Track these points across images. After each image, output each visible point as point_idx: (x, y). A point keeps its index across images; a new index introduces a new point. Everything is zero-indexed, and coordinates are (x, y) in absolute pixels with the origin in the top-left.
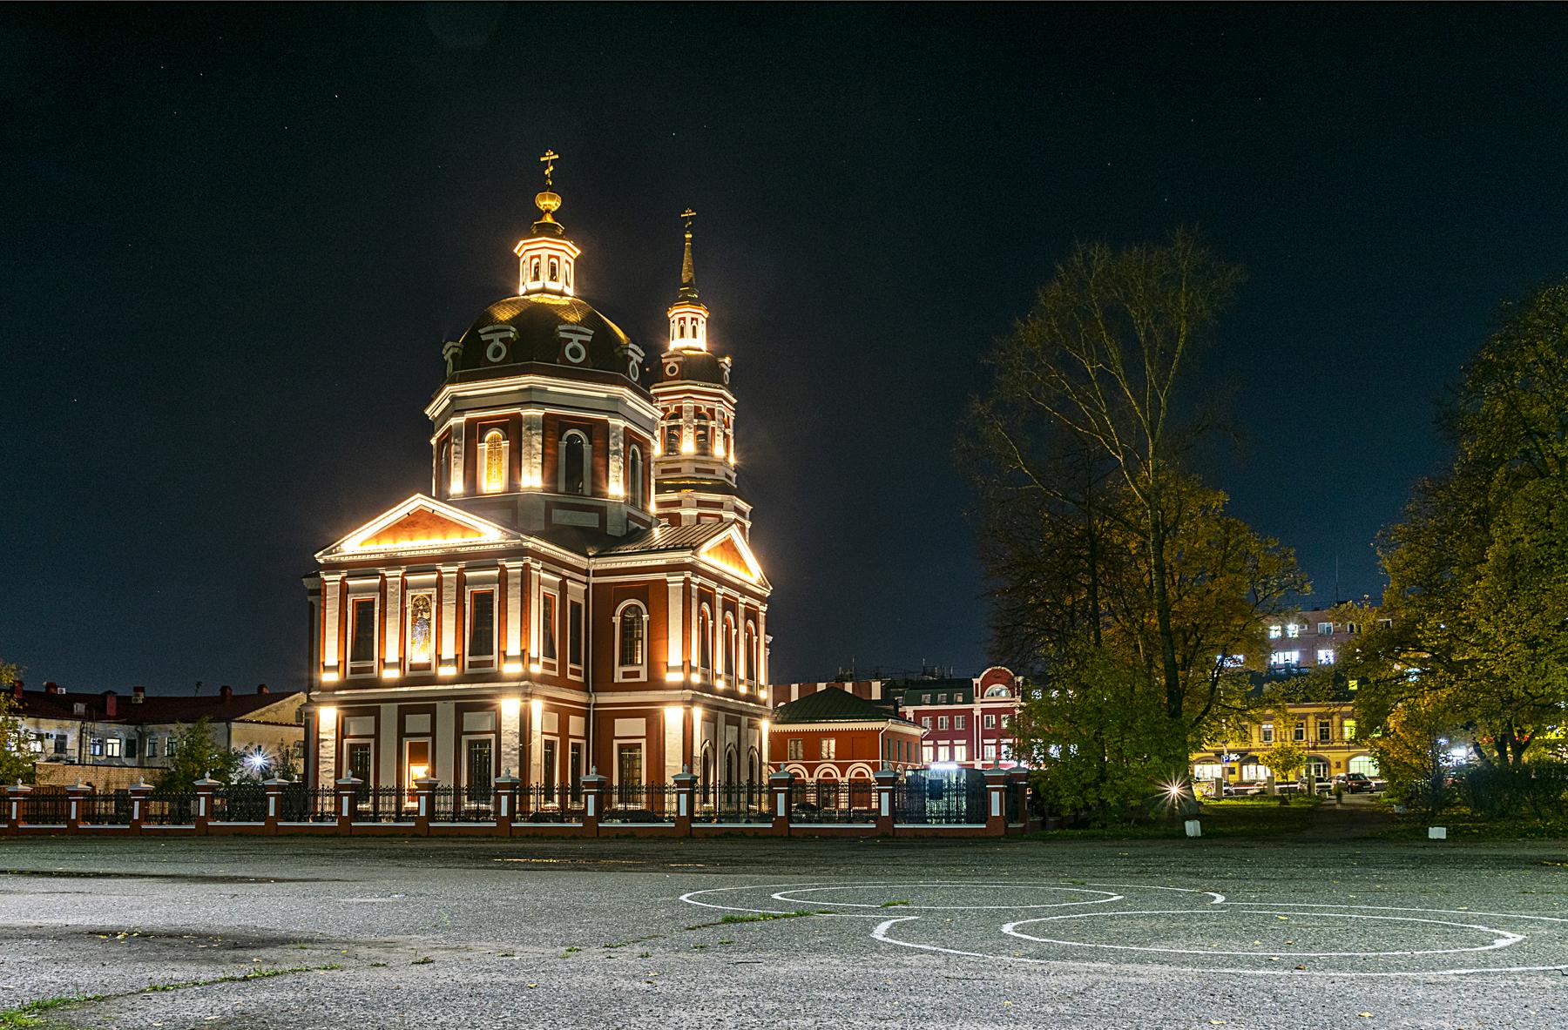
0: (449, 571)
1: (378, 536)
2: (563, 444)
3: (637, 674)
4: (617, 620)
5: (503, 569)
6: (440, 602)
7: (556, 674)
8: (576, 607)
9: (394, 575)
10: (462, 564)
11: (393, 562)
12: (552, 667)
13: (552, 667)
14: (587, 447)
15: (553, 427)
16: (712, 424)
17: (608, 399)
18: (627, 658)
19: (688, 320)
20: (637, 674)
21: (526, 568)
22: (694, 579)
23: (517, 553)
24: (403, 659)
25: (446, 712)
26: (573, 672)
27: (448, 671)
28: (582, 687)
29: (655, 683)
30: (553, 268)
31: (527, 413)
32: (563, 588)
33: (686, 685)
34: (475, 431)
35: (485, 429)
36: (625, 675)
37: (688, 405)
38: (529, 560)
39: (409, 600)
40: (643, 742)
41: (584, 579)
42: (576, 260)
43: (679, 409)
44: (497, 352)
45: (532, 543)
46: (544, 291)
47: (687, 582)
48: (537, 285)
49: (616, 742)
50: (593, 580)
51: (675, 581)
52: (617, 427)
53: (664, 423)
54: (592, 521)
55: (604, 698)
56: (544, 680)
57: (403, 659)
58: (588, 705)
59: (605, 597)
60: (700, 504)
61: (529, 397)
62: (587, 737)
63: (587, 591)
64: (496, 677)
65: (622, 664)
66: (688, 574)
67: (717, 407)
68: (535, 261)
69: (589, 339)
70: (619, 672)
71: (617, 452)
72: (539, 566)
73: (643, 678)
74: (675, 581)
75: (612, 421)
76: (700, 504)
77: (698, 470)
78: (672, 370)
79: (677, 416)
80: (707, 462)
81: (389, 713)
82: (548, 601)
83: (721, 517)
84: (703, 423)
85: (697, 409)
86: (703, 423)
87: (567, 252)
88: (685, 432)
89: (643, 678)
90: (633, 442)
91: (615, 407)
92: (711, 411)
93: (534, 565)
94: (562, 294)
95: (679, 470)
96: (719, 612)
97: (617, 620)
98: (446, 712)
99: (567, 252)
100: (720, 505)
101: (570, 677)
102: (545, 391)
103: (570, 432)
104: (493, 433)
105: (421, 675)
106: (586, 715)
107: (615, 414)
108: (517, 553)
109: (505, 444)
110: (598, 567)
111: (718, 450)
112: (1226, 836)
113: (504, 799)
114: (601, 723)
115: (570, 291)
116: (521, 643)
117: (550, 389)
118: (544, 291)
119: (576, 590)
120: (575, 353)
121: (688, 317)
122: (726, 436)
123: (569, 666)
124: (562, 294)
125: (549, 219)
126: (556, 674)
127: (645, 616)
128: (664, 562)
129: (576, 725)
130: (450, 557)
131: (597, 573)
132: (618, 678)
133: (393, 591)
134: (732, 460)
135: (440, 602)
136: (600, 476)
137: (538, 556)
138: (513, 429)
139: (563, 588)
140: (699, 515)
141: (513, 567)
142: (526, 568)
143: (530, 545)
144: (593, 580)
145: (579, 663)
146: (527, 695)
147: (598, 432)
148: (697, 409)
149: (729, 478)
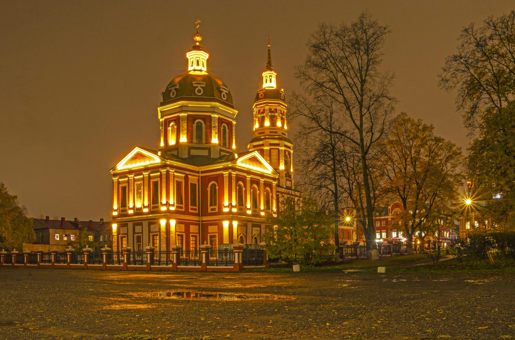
0: (146, 174)
1: (127, 164)
2: (195, 125)
5: (161, 172)
6: (144, 186)
7: (183, 210)
8: (193, 186)
9: (131, 176)
10: (149, 171)
11: (131, 172)
12: (182, 208)
13: (182, 208)
14: (204, 126)
15: (191, 119)
16: (276, 114)
17: (211, 107)
18: (213, 203)
19: (268, 77)
20: (214, 209)
21: (168, 172)
22: (233, 173)
23: (164, 166)
24: (134, 206)
25: (145, 224)
26: (191, 209)
27: (146, 210)
28: (197, 215)
30: (198, 62)
31: (182, 115)
32: (186, 178)
33: (230, 212)
34: (167, 123)
35: (170, 122)
36: (212, 210)
37: (267, 108)
38: (168, 168)
39: (135, 185)
40: (217, 234)
41: (198, 175)
42: (207, 60)
43: (264, 110)
44: (174, 93)
45: (169, 162)
46: (195, 70)
47: (230, 174)
48: (192, 68)
49: (209, 235)
50: (201, 175)
51: (226, 173)
52: (215, 117)
53: (259, 115)
54: (205, 153)
55: (205, 218)
56: (176, 212)
57: (134, 206)
58: (199, 221)
59: (205, 181)
60: (271, 145)
61: (182, 109)
63: (199, 179)
64: (160, 212)
65: (211, 205)
66: (230, 171)
67: (279, 108)
68: (192, 60)
69: (204, 86)
70: (210, 208)
71: (214, 127)
72: (173, 171)
73: (217, 211)
74: (226, 173)
75: (213, 115)
76: (271, 145)
77: (271, 132)
78: (261, 95)
79: (263, 112)
80: (264, 129)
81: (130, 225)
82: (179, 184)
83: (279, 149)
84: (273, 114)
85: (270, 109)
86: (273, 114)
87: (203, 56)
88: (266, 118)
89: (217, 211)
90: (223, 122)
91: (214, 110)
92: (276, 110)
93: (170, 170)
94: (201, 71)
95: (264, 133)
96: (248, 185)
98: (145, 224)
99: (203, 56)
100: (278, 145)
101: (190, 211)
102: (187, 106)
103: (197, 121)
104: (172, 124)
105: (138, 211)
106: (199, 225)
107: (214, 112)
108: (164, 166)
109: (175, 127)
110: (203, 170)
111: (279, 124)
113: (204, 255)
114: (204, 227)
115: (205, 69)
116: (169, 200)
117: (189, 105)
118: (195, 70)
119: (193, 179)
120: (199, 91)
121: (268, 75)
122: (282, 119)
123: (190, 207)
124: (201, 71)
125: (198, 44)
126: (183, 210)
128: (222, 167)
129: (193, 229)
130: (146, 169)
131: (202, 172)
132: (209, 211)
133: (131, 182)
134: (286, 127)
135: (144, 186)
136: (209, 137)
137: (172, 167)
138: (177, 120)
139: (186, 178)
140: (270, 149)
141: (164, 171)
142: (168, 172)
143: (168, 163)
144: (201, 175)
145: (195, 206)
146: (168, 219)
147: (208, 120)
148: (270, 109)
149: (284, 134)
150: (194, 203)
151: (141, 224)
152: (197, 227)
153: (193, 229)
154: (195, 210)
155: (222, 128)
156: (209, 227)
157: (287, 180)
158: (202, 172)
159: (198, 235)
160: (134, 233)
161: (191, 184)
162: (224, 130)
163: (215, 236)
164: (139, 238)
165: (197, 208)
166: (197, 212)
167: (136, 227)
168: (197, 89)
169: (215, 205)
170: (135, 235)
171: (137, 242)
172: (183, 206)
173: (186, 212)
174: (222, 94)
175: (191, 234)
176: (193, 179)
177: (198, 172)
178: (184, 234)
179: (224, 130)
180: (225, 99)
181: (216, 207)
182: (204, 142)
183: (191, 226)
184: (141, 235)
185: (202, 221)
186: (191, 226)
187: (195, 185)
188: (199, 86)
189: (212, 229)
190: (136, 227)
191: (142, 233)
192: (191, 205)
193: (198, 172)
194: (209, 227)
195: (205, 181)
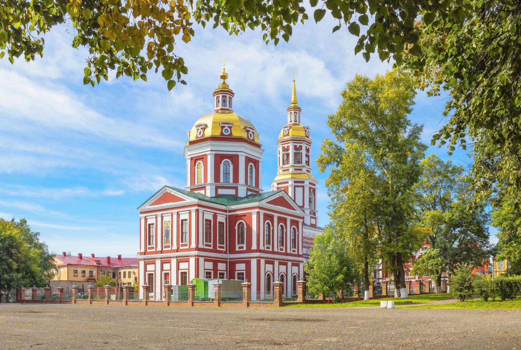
3: (242, 247)
4: (236, 228)
8: (221, 223)
12: (210, 246)
20: (242, 247)
26: (220, 247)
29: (249, 250)
32: (215, 216)
36: (240, 248)
40: (244, 272)
41: (226, 214)
49: (236, 272)
50: (228, 214)
58: (227, 259)
62: (226, 270)
63: (226, 218)
73: (245, 249)
97: (236, 228)
101: (218, 249)
106: (226, 262)
112: (291, 304)
119: (221, 218)
123: (218, 245)
126: (212, 248)
127: (245, 226)
129: (222, 267)
131: (230, 211)
132: (237, 249)
139: (215, 216)
144: (228, 214)
145: (223, 244)
150: (222, 242)
151: (169, 262)
152: (224, 265)
153: (222, 267)
154: (223, 248)
155: (249, 167)
156: (237, 265)
157: (311, 217)
158: (230, 211)
159: (225, 272)
160: (162, 269)
161: (219, 222)
162: (251, 169)
163: (243, 274)
164: (167, 275)
165: (225, 246)
166: (224, 250)
167: (164, 265)
168: (224, 129)
169: (243, 243)
170: (163, 272)
171: (165, 278)
172: (212, 244)
173: (215, 251)
174: (249, 133)
175: (219, 272)
176: (221, 218)
177: (226, 211)
178: (212, 271)
179: (251, 169)
180: (252, 139)
181: (245, 246)
182: (231, 181)
183: (219, 264)
184: (169, 272)
185: (230, 259)
186: (219, 264)
187: (223, 223)
188: (227, 126)
189: (241, 267)
190: (164, 265)
191: (170, 270)
192: (220, 243)
193: (226, 211)
194: (237, 265)
195: (233, 219)
